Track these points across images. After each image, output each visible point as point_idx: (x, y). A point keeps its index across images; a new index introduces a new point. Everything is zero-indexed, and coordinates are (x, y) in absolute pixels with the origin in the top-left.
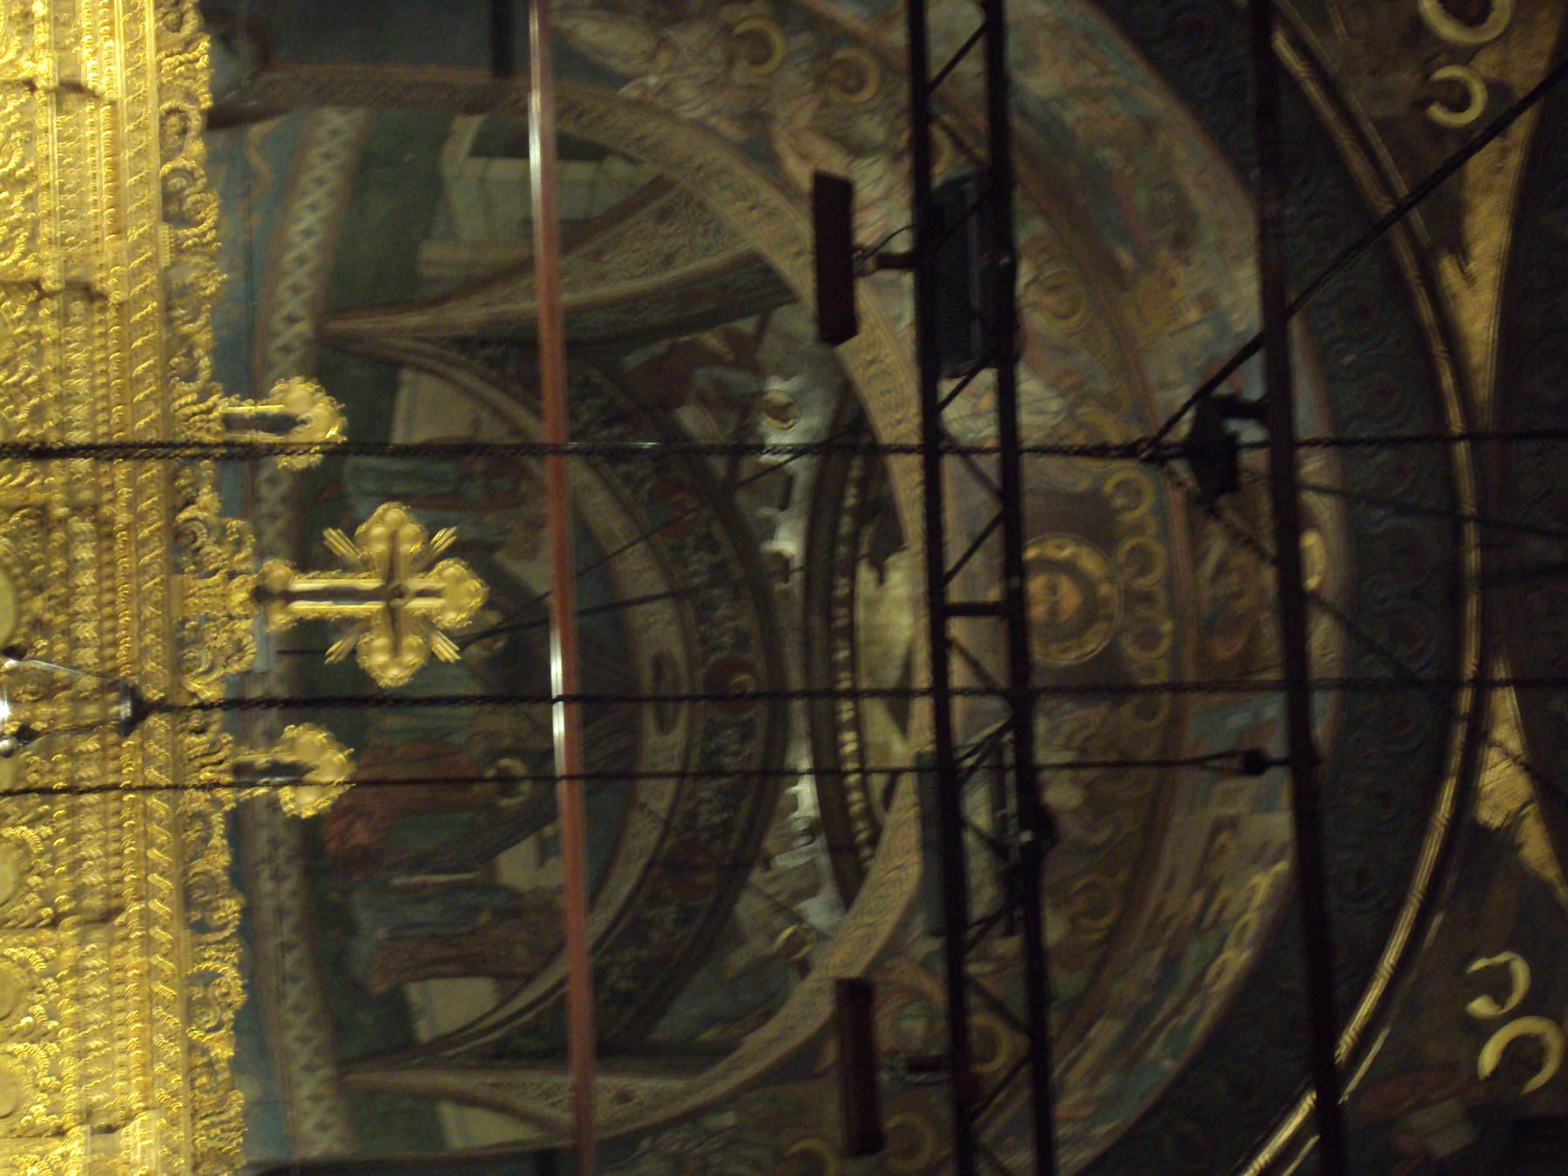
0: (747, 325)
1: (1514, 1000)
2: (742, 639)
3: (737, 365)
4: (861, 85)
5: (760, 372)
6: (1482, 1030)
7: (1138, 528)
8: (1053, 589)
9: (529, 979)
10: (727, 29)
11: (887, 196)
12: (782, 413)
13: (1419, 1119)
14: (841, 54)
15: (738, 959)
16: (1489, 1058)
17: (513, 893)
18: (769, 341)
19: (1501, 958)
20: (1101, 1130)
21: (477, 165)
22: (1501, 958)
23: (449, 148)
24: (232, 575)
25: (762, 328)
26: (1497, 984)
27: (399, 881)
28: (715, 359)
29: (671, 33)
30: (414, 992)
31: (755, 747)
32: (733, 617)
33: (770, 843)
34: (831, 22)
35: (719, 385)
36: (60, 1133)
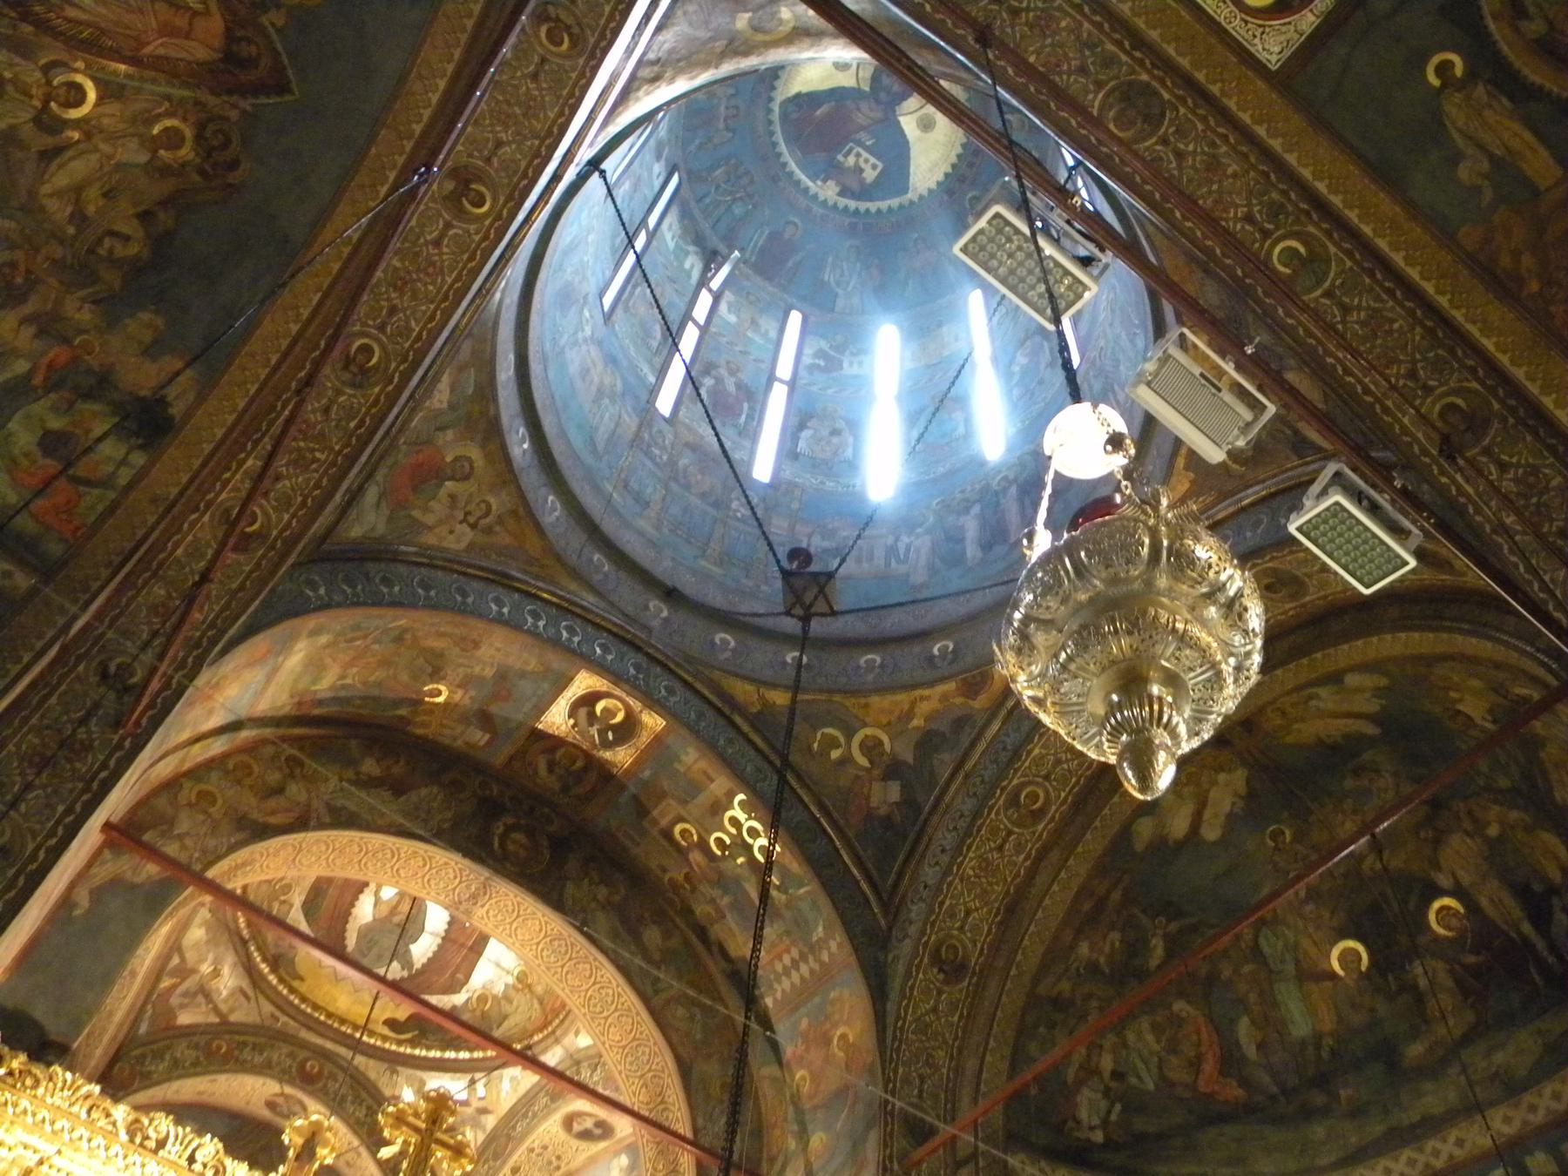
0: (176, 960)
1: (842, 740)
2: (291, 1055)
3: (183, 980)
4: (249, 767)
5: (194, 971)
6: (846, 760)
8: (514, 842)
10: (190, 805)
11: (309, 792)
12: (216, 973)
13: (874, 802)
14: (231, 766)
16: (863, 761)
19: (819, 736)
22: (819, 736)
26: (832, 743)
28: (175, 986)
31: (341, 1077)
32: (279, 1054)
35: (185, 994)
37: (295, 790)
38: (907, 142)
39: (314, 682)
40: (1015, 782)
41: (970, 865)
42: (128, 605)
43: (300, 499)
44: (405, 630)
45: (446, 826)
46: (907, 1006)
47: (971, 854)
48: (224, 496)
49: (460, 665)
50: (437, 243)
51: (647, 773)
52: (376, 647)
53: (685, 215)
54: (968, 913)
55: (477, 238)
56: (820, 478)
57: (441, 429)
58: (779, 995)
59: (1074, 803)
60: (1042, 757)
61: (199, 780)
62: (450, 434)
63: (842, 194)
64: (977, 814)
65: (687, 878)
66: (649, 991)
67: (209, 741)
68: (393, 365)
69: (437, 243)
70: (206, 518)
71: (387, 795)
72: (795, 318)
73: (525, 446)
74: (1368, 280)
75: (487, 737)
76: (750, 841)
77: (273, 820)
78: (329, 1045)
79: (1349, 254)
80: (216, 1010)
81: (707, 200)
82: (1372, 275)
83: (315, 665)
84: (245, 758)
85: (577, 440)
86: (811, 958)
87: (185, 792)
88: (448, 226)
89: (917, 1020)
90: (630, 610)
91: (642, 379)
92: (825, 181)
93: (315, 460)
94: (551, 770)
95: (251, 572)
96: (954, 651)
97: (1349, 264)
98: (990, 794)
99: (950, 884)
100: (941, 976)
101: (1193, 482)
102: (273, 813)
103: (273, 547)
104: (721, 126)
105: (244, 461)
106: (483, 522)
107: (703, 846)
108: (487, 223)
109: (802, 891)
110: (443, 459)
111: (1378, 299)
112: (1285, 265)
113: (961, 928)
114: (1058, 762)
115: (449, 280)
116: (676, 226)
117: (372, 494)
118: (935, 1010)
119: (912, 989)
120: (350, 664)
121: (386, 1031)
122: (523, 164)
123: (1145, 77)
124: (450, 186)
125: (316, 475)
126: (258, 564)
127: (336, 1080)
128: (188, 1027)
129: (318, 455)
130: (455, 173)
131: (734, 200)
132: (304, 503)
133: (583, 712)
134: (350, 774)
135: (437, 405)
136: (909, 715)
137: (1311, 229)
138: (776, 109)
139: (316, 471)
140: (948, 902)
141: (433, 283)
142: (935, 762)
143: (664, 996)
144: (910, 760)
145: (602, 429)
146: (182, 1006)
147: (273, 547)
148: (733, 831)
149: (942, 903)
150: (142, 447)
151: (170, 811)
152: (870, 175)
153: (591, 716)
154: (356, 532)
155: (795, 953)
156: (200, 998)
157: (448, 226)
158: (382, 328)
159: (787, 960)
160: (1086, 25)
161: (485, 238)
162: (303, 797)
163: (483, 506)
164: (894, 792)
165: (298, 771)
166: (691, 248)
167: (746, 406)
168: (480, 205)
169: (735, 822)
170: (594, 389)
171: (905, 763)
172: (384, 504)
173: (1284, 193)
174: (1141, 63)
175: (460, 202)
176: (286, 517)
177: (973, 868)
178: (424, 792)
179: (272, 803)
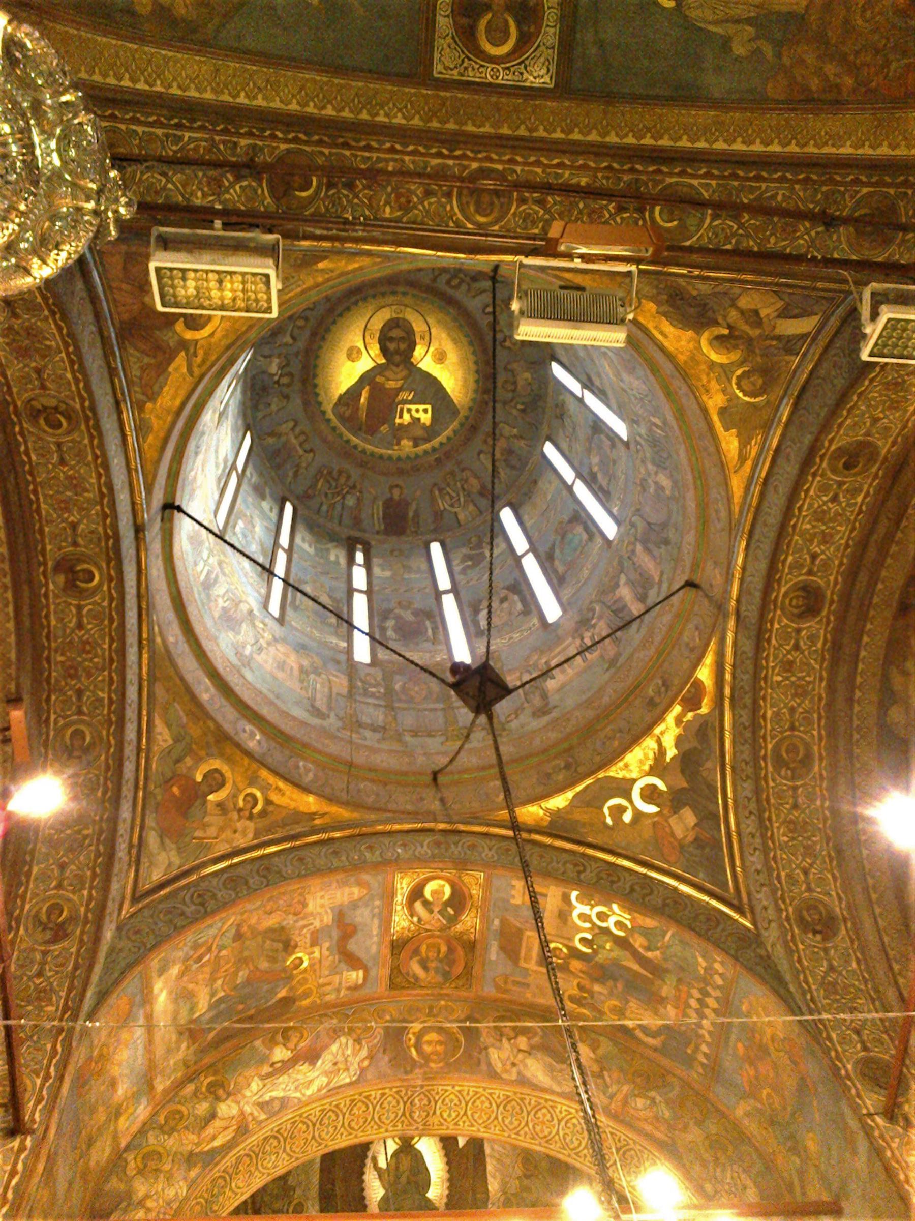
1: (623, 802)
4: (180, 1112)
6: (638, 816)
8: (429, 1043)
11: (238, 1103)
13: (679, 834)
16: (652, 809)
26: (618, 811)
34: (144, 1124)
38: (435, 378)
39: (192, 1010)
40: (770, 746)
41: (781, 835)
43: (89, 873)
44: (239, 926)
45: (366, 1063)
46: (805, 977)
47: (776, 825)
48: (27, 907)
49: (305, 926)
50: (80, 626)
51: (497, 922)
52: (224, 953)
53: (312, 527)
54: (806, 872)
55: (105, 604)
56: (507, 637)
57: (178, 761)
58: (708, 1038)
59: (829, 735)
60: (777, 714)
62: (188, 761)
63: (416, 445)
64: (757, 791)
65: (581, 987)
68: (104, 733)
69: (80, 626)
70: (22, 931)
71: (305, 1067)
72: (436, 548)
73: (258, 737)
74: (736, 183)
75: (361, 973)
76: (604, 925)
77: (217, 1143)
79: (707, 175)
81: (324, 508)
82: (735, 176)
83: (183, 996)
85: (298, 712)
86: (709, 989)
87: (132, 1164)
88: (79, 608)
89: (822, 984)
90: (409, 807)
91: (335, 649)
92: (398, 443)
93: (86, 837)
94: (425, 968)
95: (78, 951)
96: (664, 685)
97: (714, 183)
98: (757, 767)
99: (774, 858)
100: (819, 937)
101: (738, 435)
102: (214, 1138)
103: (86, 922)
104: (301, 452)
106: (255, 811)
107: (575, 953)
108: (105, 588)
109: (667, 937)
110: (194, 781)
111: (752, 190)
112: (671, 221)
113: (809, 889)
114: (792, 710)
115: (106, 646)
116: (308, 537)
117: (152, 839)
118: (832, 968)
119: (799, 961)
120: (213, 980)
122: (101, 529)
123: (475, 165)
124: (61, 579)
125: (93, 848)
126: (81, 941)
129: (86, 832)
130: (57, 568)
131: (344, 498)
132: (94, 875)
133: (418, 905)
134: (266, 1069)
135: (165, 745)
136: (661, 751)
137: (670, 180)
138: (332, 417)
140: (783, 874)
141: (96, 656)
142: (704, 774)
143: (619, 1097)
144: (685, 785)
145: (318, 696)
147: (86, 922)
148: (588, 925)
149: (779, 878)
151: (122, 1187)
152: (426, 418)
153: (426, 904)
154: (157, 876)
155: (696, 993)
157: (79, 608)
158: (80, 712)
159: (693, 1003)
160: (407, 158)
161: (111, 599)
162: (235, 1111)
163: (249, 798)
164: (689, 817)
165: (220, 1092)
166: (330, 546)
167: (428, 623)
168: (92, 579)
169: (584, 917)
170: (296, 672)
171: (683, 789)
172: (167, 841)
173: (632, 170)
174: (464, 157)
175: (77, 586)
176: (86, 892)
177: (784, 835)
178: (334, 1048)
179: (210, 1131)
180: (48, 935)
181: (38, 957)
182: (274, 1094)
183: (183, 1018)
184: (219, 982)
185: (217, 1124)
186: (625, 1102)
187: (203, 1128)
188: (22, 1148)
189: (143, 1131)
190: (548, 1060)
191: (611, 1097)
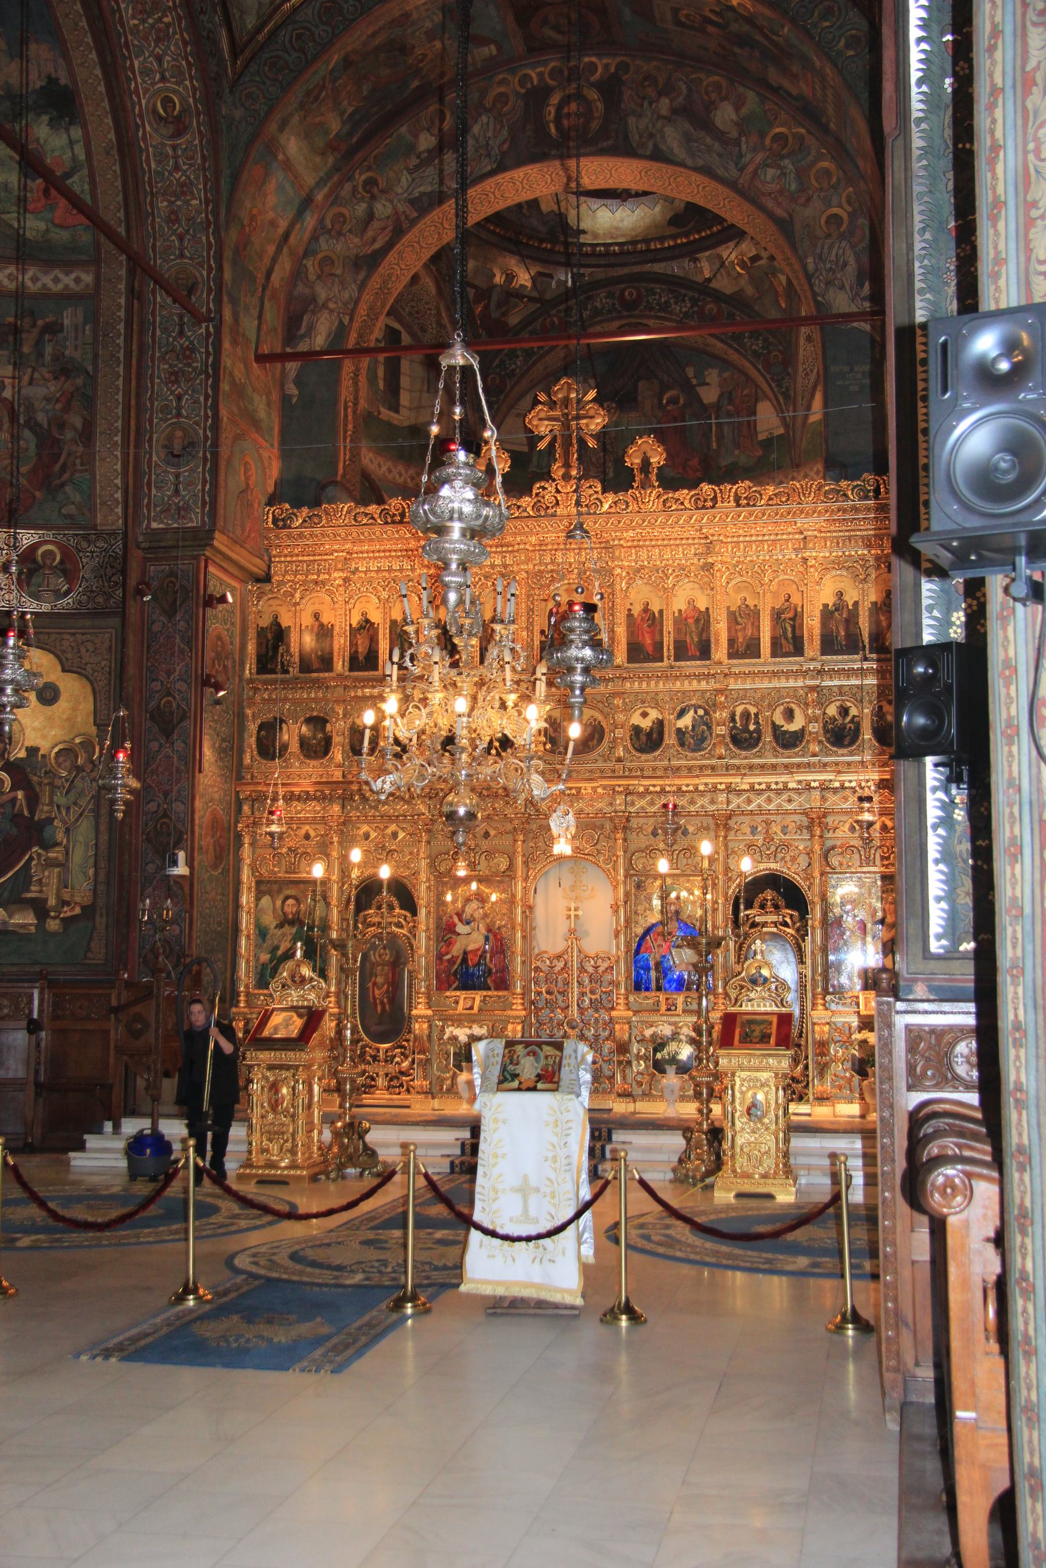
0: (471, 292)
2: (610, 295)
4: (342, 215)
7: (540, 75)
9: (757, 386)
12: (510, 277)
15: (750, 291)
17: (721, 396)
18: (477, 283)
20: (818, 64)
21: (402, 411)
23: (396, 422)
24: (558, 491)
25: (474, 286)
27: (714, 446)
28: (486, 307)
29: (320, 302)
30: (761, 437)
31: (657, 287)
32: (601, 300)
33: (699, 279)
34: (315, 230)
35: (499, 305)
36: (805, 560)
37: (383, 208)
42: (153, 228)
45: (506, 147)
48: (144, 102)
61: (314, 253)
66: (734, 172)
67: (298, 226)
70: (148, 128)
75: (493, 47)
77: (377, 245)
78: (636, 269)
80: (531, 299)
84: (336, 210)
87: (311, 269)
93: (168, 25)
95: (201, 142)
102: (374, 240)
105: (132, 65)
121: (673, 230)
125: (177, 36)
126: (200, 132)
127: (655, 294)
128: (520, 322)
129: (166, 20)
139: (175, 33)
146: (504, 314)
150: (71, 123)
151: (307, 291)
154: (251, 22)
156: (514, 300)
165: (375, 190)
176: (187, 83)
179: (370, 233)
180: (171, 129)
181: (170, 152)
182: (422, 189)
183: (320, 142)
184: (345, 103)
185: (376, 225)
186: (755, 174)
187: (364, 230)
188: (208, 334)
189: (314, 238)
190: (687, 126)
191: (741, 170)
